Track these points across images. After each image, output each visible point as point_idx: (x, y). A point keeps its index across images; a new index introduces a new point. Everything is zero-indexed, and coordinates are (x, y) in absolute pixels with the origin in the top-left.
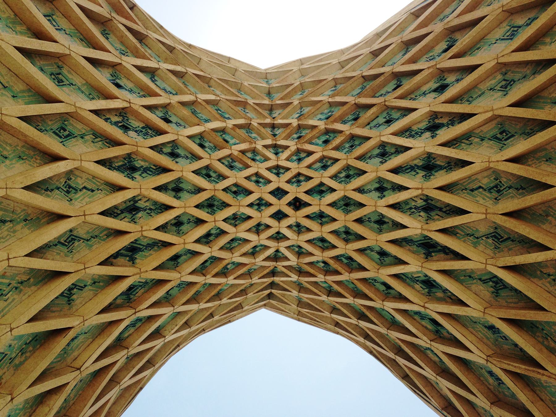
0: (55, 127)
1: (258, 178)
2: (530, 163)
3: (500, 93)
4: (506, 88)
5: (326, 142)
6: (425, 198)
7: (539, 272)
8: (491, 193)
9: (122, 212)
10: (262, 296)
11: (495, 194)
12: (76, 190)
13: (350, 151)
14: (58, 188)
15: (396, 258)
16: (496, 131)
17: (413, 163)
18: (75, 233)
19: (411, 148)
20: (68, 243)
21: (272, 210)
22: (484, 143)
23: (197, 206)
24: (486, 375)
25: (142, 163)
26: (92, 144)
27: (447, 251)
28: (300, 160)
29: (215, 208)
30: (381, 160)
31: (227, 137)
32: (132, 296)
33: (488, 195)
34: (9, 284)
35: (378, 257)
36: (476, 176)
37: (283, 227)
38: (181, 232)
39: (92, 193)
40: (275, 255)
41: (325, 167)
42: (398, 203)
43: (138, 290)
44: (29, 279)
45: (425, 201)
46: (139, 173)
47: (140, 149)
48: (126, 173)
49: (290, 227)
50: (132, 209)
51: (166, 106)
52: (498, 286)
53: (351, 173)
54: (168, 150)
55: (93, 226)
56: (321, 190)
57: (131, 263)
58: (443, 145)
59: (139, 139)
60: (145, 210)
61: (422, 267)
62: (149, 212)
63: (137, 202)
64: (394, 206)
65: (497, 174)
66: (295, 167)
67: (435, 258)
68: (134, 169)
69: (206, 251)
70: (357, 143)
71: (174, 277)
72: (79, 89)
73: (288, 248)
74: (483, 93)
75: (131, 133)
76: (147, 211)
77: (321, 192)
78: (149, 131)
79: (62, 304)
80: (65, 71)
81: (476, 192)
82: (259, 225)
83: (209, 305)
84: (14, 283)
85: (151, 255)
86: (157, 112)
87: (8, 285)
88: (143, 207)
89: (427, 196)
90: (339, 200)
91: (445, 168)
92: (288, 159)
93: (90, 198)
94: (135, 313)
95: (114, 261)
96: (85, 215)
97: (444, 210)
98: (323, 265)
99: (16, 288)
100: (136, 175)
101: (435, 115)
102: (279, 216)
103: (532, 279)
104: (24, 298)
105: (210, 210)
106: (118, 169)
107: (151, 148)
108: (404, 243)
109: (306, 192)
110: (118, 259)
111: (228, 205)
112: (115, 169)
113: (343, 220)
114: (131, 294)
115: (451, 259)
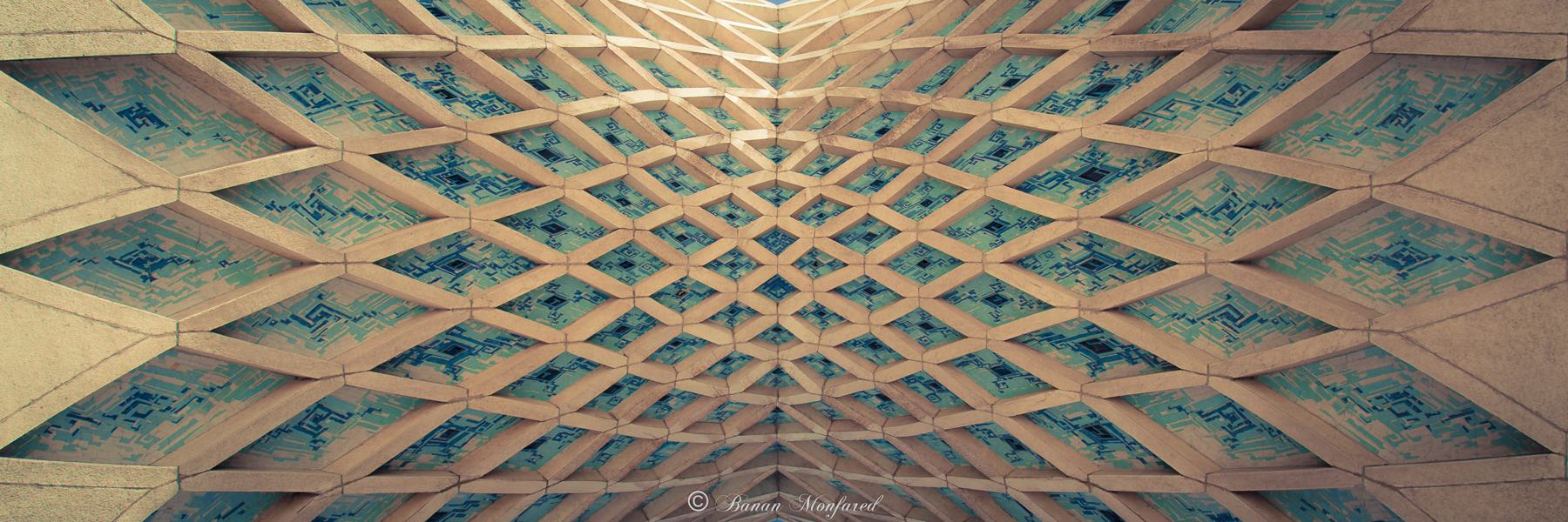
0: (295, 85)
1: (733, 211)
2: (1289, 148)
5: (882, 132)
6: (1087, 241)
7: (1313, 386)
9: (432, 269)
10: (757, 480)
11: (1225, 223)
12: (334, 214)
13: (927, 150)
14: (296, 207)
15: (1030, 378)
16: (1223, 88)
17: (1060, 167)
18: (328, 301)
19: (1055, 133)
21: (762, 276)
22: (1200, 114)
23: (595, 264)
25: (480, 169)
26: (373, 123)
27: (1135, 356)
28: (825, 171)
29: (636, 270)
30: (995, 164)
31: (670, 125)
32: (453, 450)
33: (1211, 224)
35: (995, 378)
36: (1186, 187)
37: (786, 313)
38: (560, 320)
39: (367, 223)
40: (776, 381)
41: (878, 184)
42: (1031, 256)
43: (466, 438)
44: (229, 384)
45: (1088, 247)
46: (473, 188)
47: (471, 137)
48: (443, 188)
49: (800, 314)
50: (453, 261)
51: (536, 56)
53: (934, 194)
54: (537, 143)
55: (367, 291)
56: (868, 233)
57: (450, 378)
58: (1120, 122)
59: (474, 119)
61: (1081, 393)
63: (464, 249)
64: (1020, 262)
65: (1227, 178)
66: (812, 187)
67: (1108, 373)
68: (460, 180)
69: (616, 364)
70: (946, 130)
71: (544, 413)
72: (353, 13)
73: (802, 361)
75: (459, 107)
77: (870, 237)
78: (497, 103)
79: (300, 447)
81: (1187, 220)
82: (734, 310)
83: (629, 486)
84: (195, 390)
85: (493, 363)
86: (517, 68)
88: (476, 259)
89: (1091, 236)
90: (906, 252)
92: (799, 169)
93: (361, 232)
94: (459, 484)
95: (413, 368)
96: (346, 263)
97: (1126, 265)
98: (879, 402)
99: (200, 400)
100: (465, 192)
101: (1101, 61)
102: (777, 287)
103: (1300, 401)
104: (215, 421)
105: (625, 274)
106: (426, 177)
107: (497, 136)
108: (1046, 344)
109: (836, 238)
111: (665, 264)
112: (419, 176)
113: (915, 295)
114: (451, 444)
115: (1142, 373)
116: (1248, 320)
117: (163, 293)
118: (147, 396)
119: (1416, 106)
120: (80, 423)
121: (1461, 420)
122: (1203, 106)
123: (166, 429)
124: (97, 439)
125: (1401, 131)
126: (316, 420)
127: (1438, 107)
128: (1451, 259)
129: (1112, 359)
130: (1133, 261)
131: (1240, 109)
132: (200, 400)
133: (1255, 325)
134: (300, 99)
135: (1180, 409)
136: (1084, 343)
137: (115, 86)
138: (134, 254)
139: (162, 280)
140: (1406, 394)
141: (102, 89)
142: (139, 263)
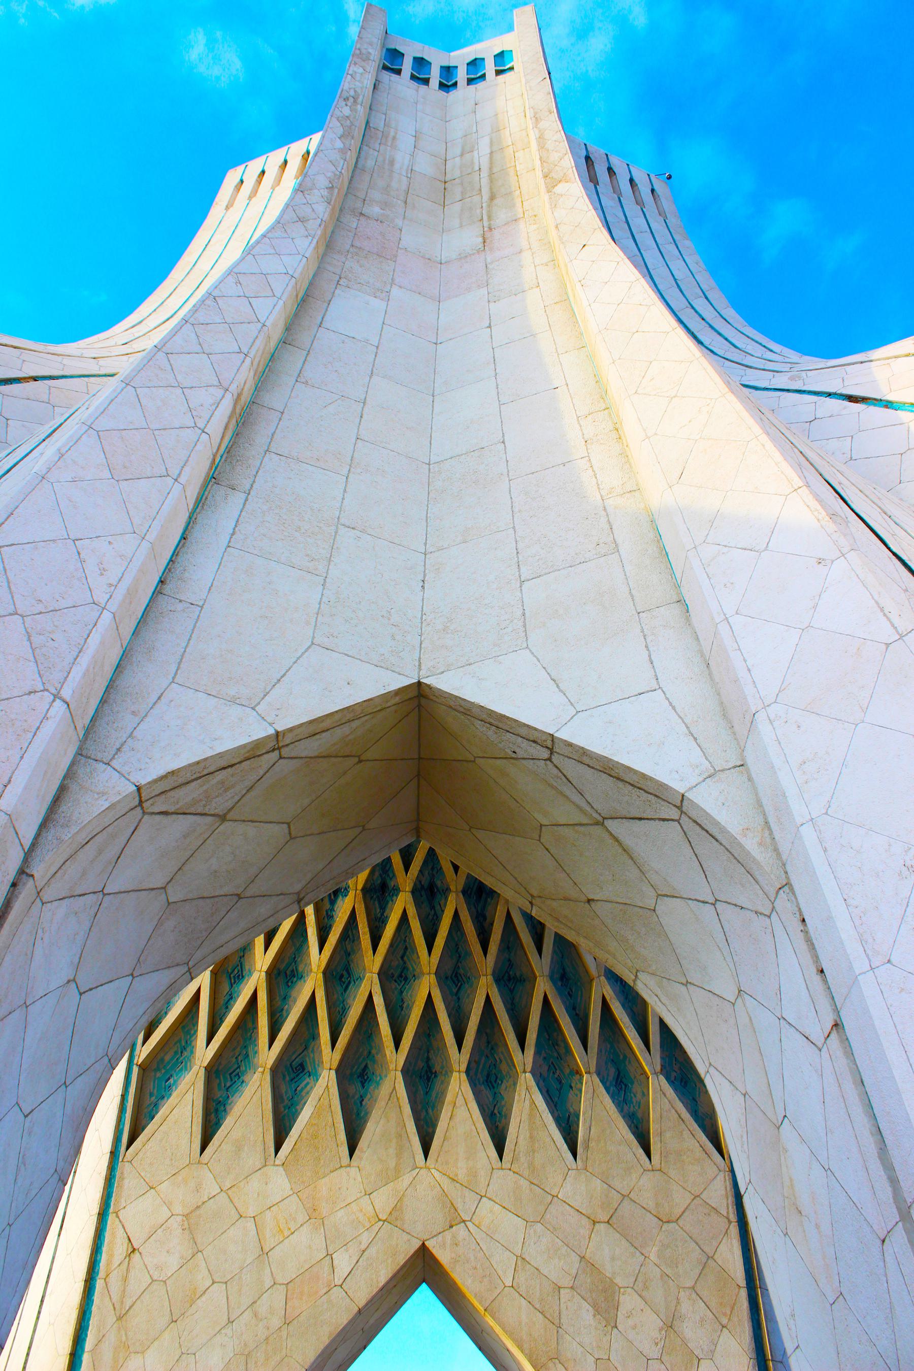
9: (433, 908)
14: (402, 992)
20: (459, 981)
25: (377, 874)
34: (487, 1056)
46: (388, 881)
48: (388, 898)
60: (433, 875)
62: (435, 870)
63: (423, 887)
76: (434, 872)
80: (282, 967)
87: (487, 1056)
99: (492, 1049)
100: (391, 884)
106: (383, 908)
110: (487, 914)
112: (382, 914)
117: (442, 1068)
118: (488, 1076)
120: (496, 1111)
123: (504, 1067)
124: (503, 1103)
126: (509, 979)
132: (492, 1049)
134: (347, 987)
137: (352, 1090)
138: (424, 1079)
139: (437, 1068)
141: (353, 1097)
142: (428, 1079)
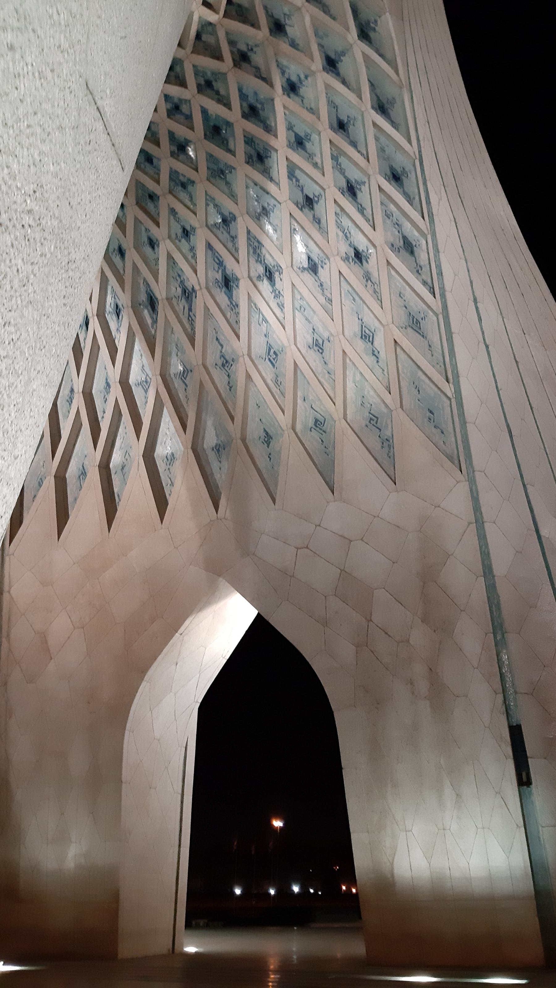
3: (310, 341)
4: (316, 345)
8: (220, 358)
11: (220, 364)
16: (275, 348)
24: (69, 389)
52: (145, 384)
74: (310, 322)
81: (217, 343)
91: (231, 303)
116: (184, 382)
119: (271, 445)
121: (170, 482)
122: (267, 339)
125: (263, 437)
127: (270, 454)
128: (220, 469)
129: (150, 314)
130: (193, 318)
131: (267, 360)
133: (184, 386)
135: (141, 355)
136: (151, 297)
140: (174, 459)
